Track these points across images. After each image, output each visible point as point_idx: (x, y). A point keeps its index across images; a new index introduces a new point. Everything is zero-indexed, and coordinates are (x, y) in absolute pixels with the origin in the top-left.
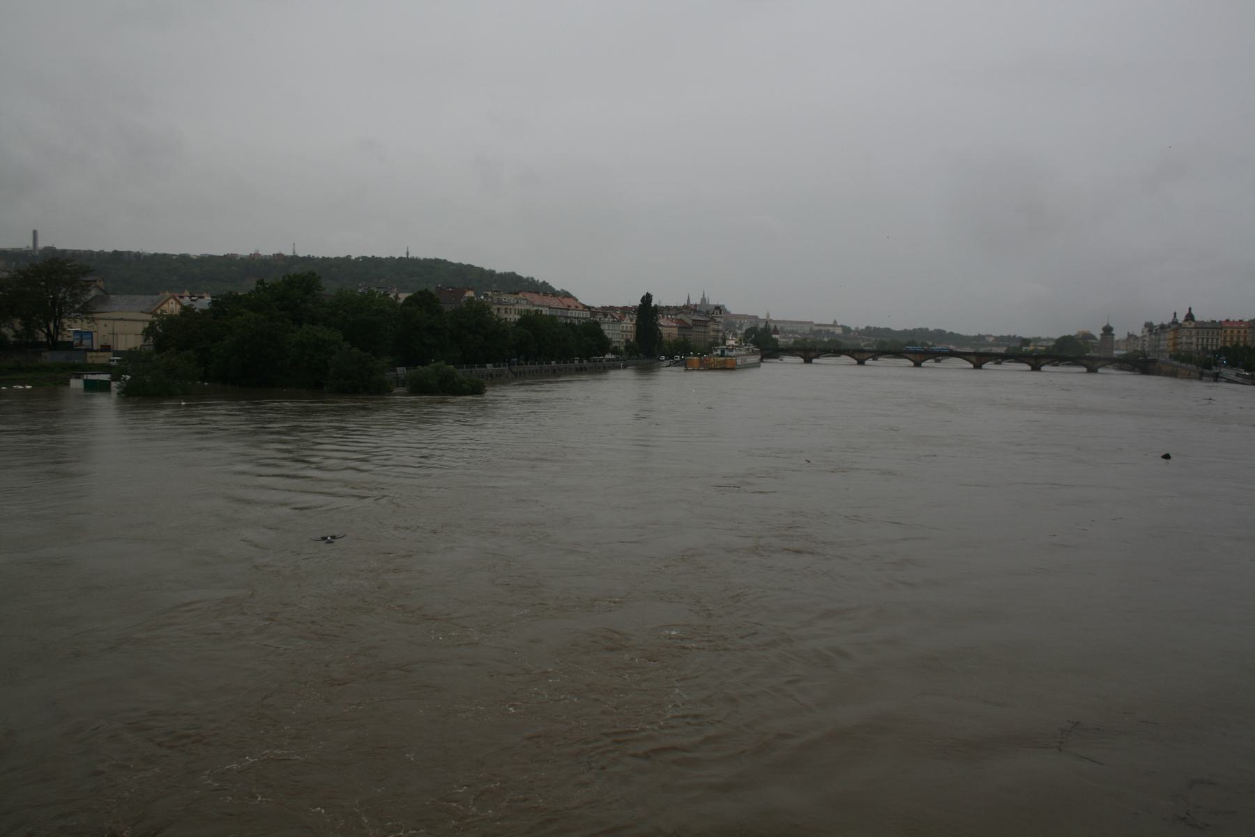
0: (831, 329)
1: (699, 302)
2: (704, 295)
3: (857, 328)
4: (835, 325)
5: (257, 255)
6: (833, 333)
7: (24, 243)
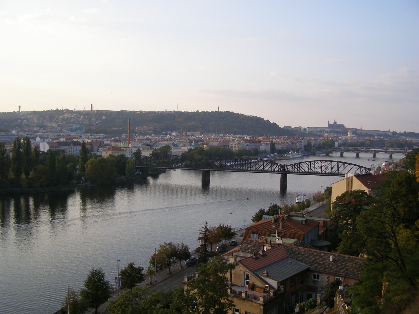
0: (387, 133)
1: (333, 123)
2: (335, 120)
4: (389, 131)
5: (166, 111)
6: (388, 135)
7: (88, 108)
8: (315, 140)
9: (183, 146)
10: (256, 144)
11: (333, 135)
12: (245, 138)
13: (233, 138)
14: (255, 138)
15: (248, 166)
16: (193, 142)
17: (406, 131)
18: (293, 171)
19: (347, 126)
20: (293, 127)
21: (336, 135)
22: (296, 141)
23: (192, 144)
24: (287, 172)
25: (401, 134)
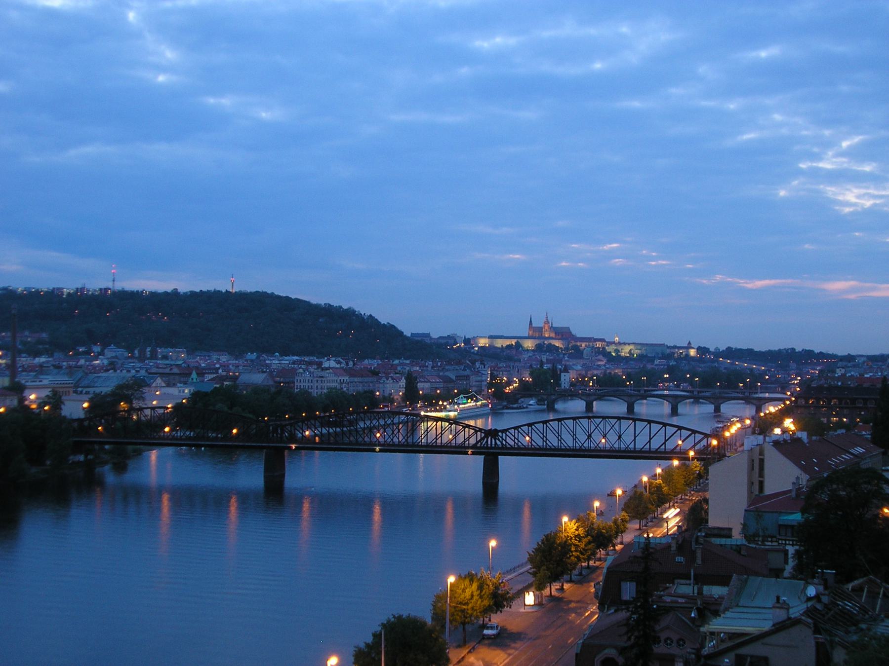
3: (717, 349)
4: (689, 346)
8: (509, 369)
9: (164, 385)
10: (366, 379)
11: (545, 356)
12: (326, 365)
13: (289, 364)
14: (351, 364)
15: (393, 433)
16: (191, 374)
17: (732, 346)
18: (516, 446)
19: (578, 332)
20: (435, 335)
21: (551, 358)
22: (468, 372)
23: (190, 380)
24: (499, 448)
25: (718, 354)
